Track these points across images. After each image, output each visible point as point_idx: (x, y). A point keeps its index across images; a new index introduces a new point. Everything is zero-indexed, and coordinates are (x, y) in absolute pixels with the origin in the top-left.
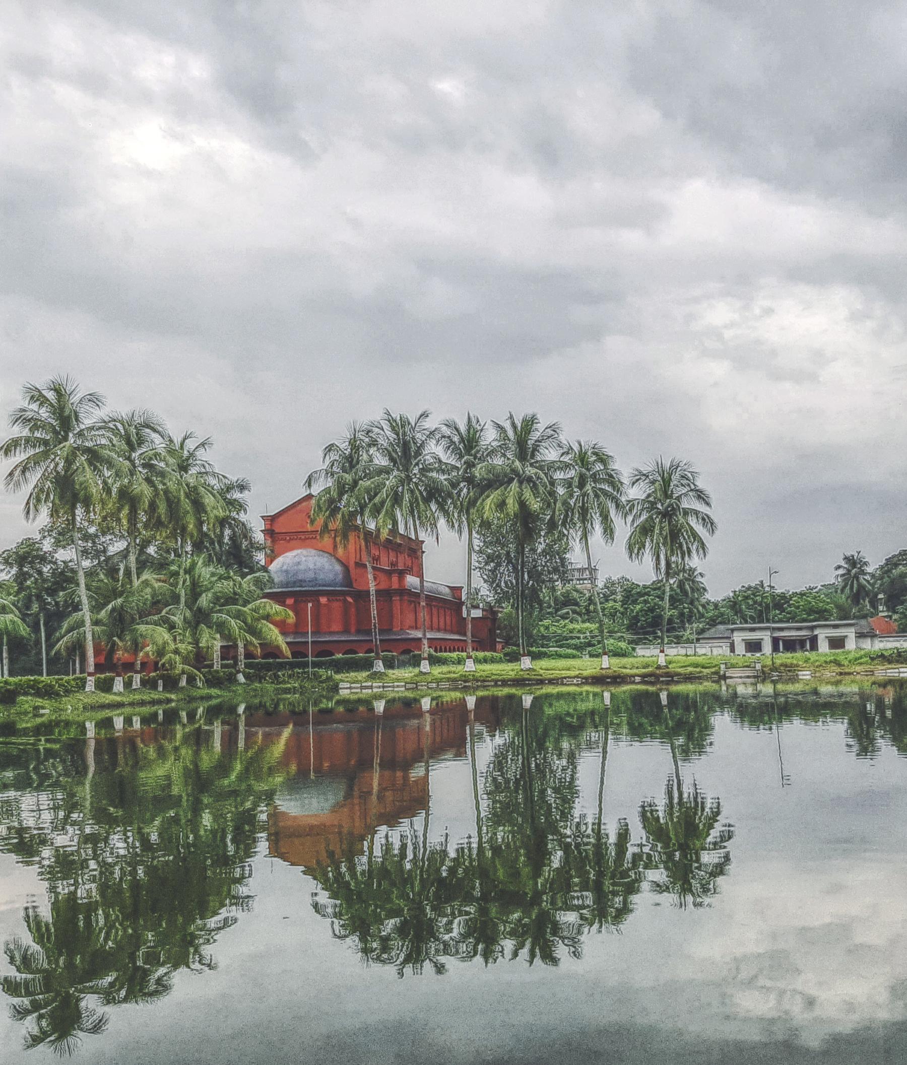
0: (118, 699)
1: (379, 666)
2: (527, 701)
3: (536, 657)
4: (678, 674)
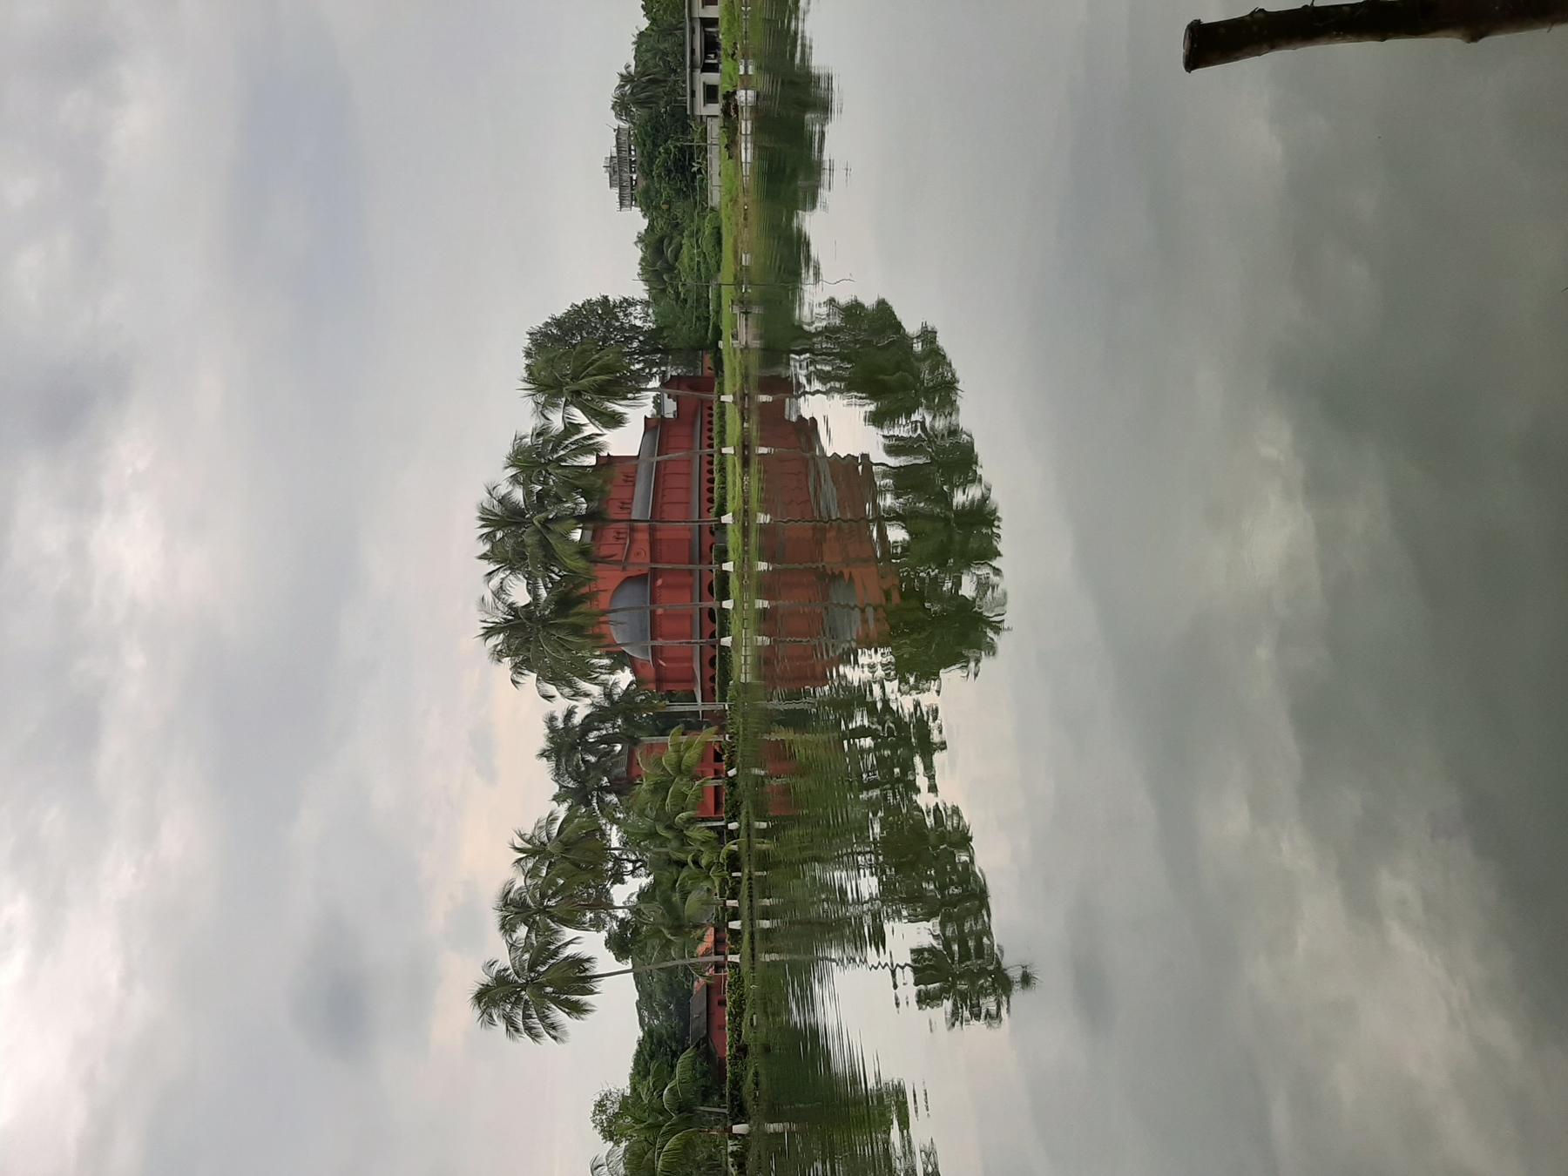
0: (748, 923)
1: (726, 641)
2: (763, 518)
3: (722, 511)
4: (742, 388)
